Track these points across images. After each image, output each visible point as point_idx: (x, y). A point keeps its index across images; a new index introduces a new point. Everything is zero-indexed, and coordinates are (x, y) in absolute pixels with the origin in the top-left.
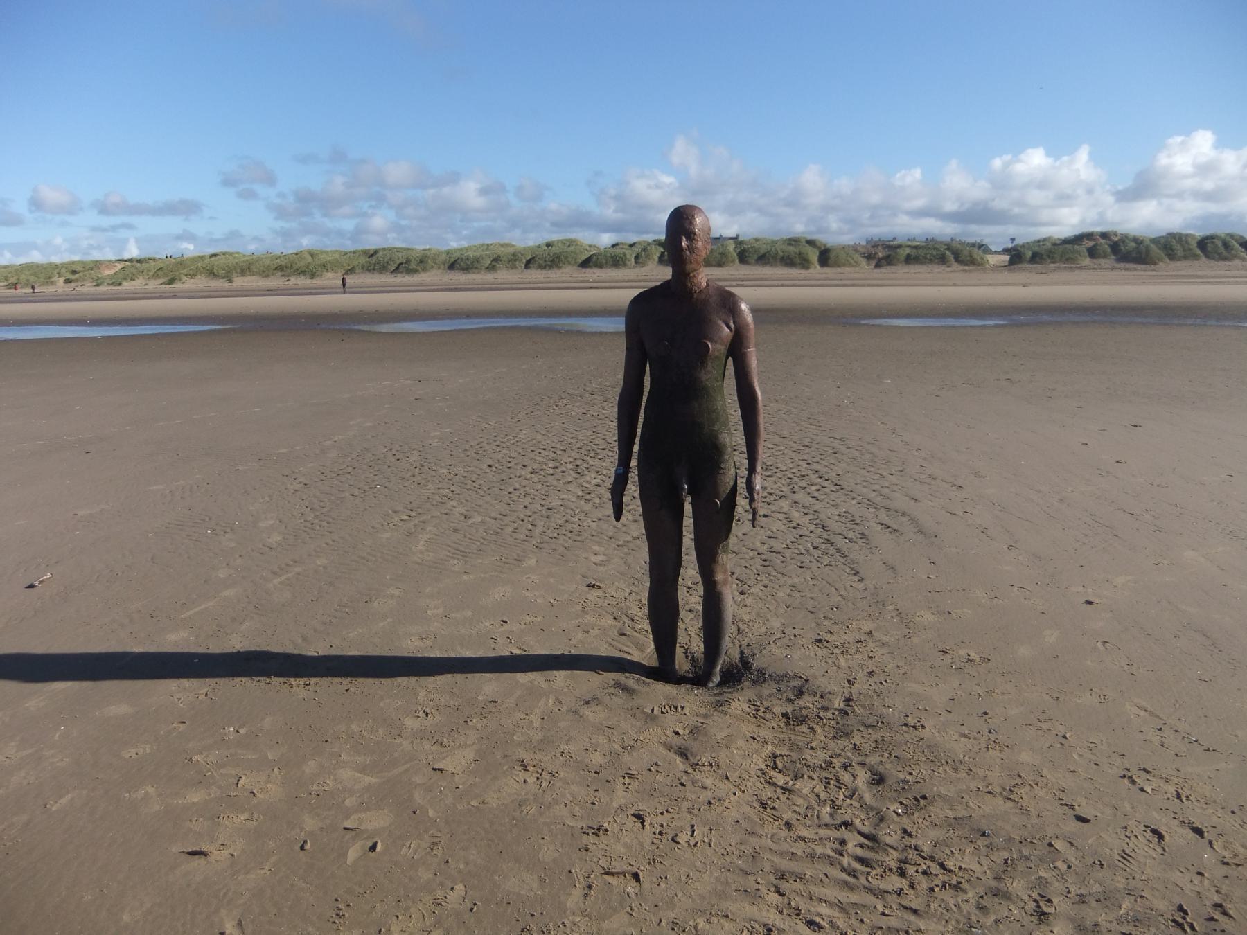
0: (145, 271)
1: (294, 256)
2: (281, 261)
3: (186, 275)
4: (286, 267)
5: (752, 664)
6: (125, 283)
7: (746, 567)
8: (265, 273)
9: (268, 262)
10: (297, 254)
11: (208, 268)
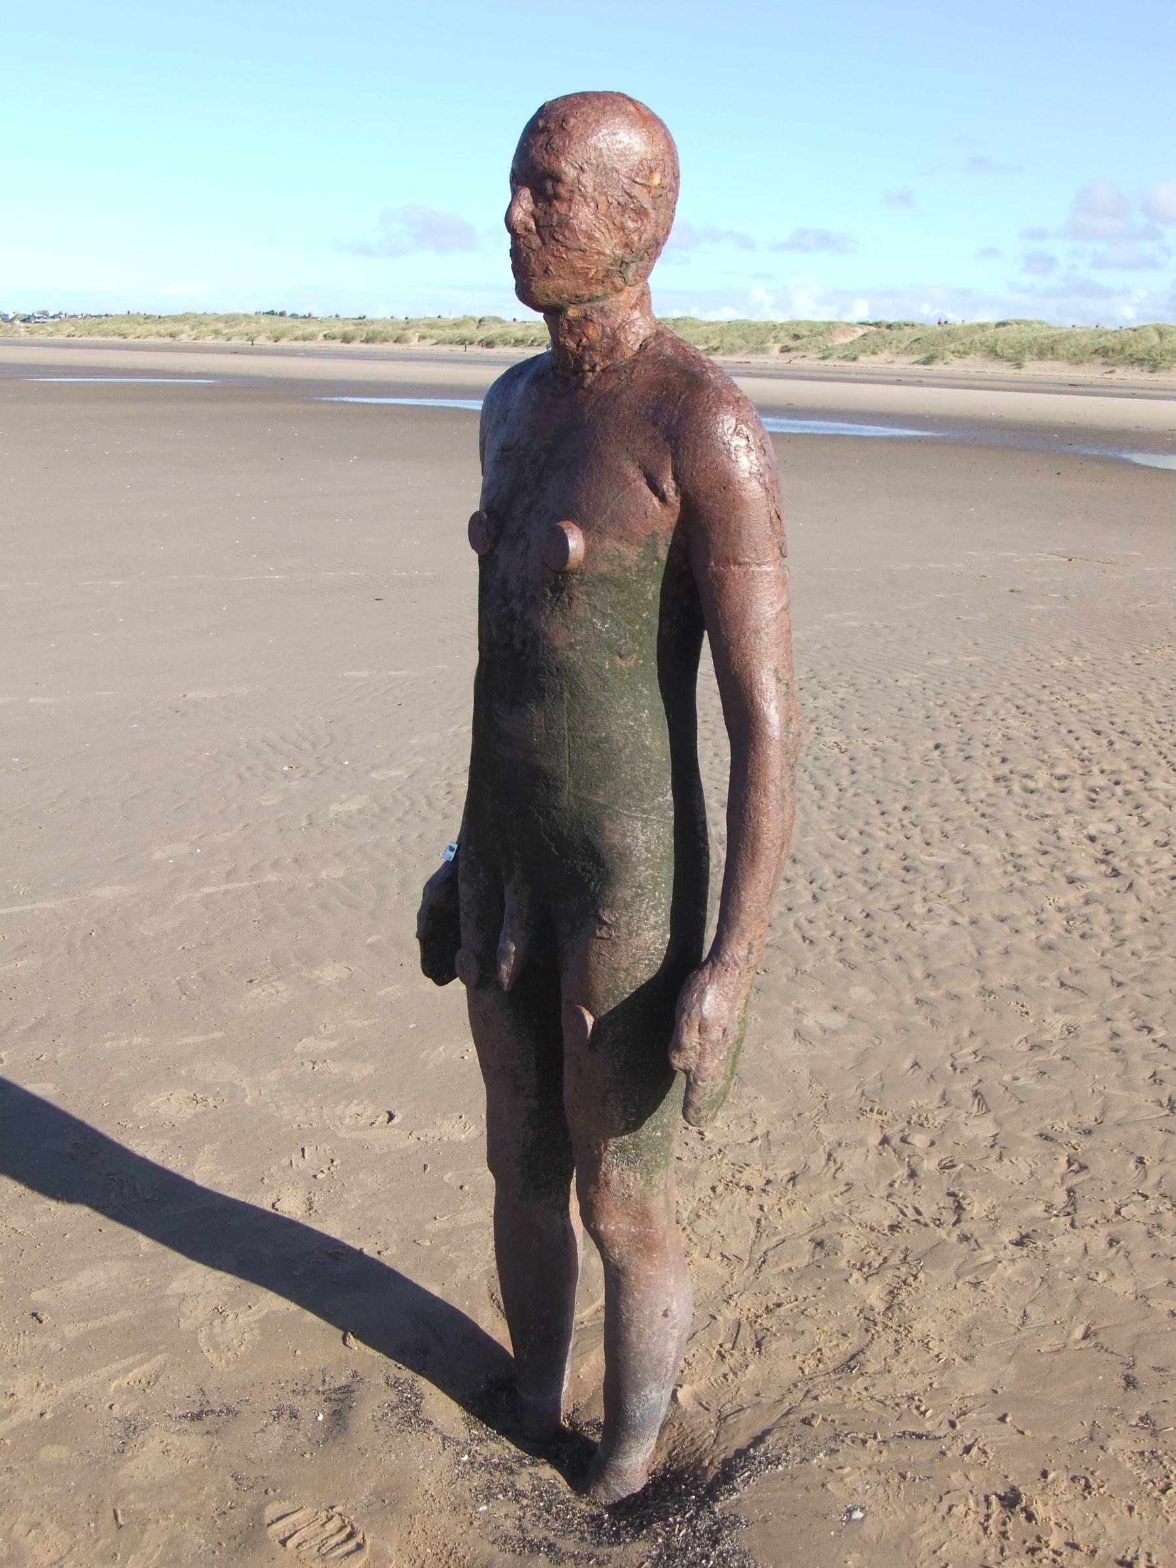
0: (894, 342)
1: (1131, 333)
2: (1106, 339)
3: (953, 353)
4: (1113, 350)
5: (735, 1490)
6: (862, 358)
7: (1141, 1161)
8: (1077, 358)
9: (1085, 340)
10: (1135, 330)
11: (987, 343)
